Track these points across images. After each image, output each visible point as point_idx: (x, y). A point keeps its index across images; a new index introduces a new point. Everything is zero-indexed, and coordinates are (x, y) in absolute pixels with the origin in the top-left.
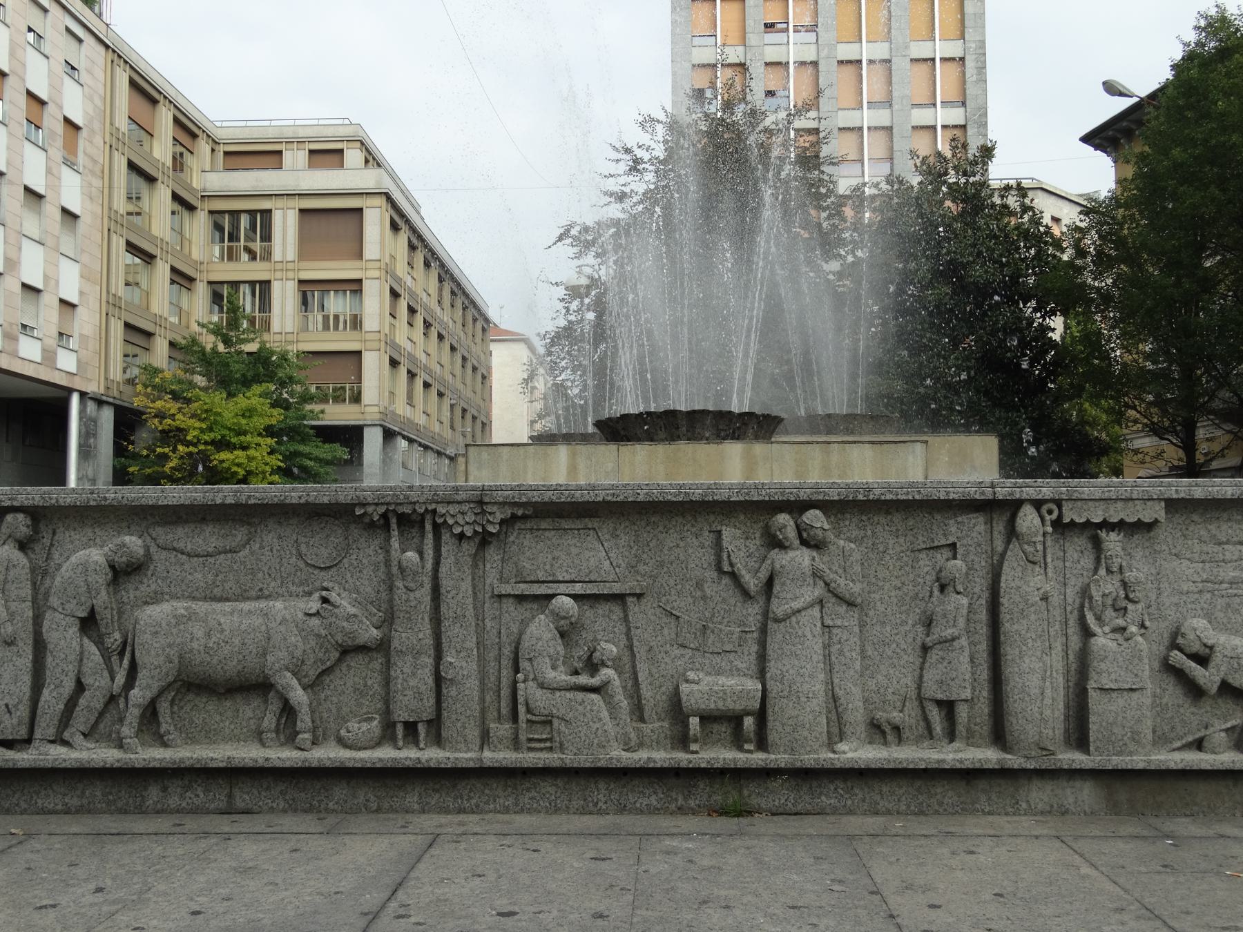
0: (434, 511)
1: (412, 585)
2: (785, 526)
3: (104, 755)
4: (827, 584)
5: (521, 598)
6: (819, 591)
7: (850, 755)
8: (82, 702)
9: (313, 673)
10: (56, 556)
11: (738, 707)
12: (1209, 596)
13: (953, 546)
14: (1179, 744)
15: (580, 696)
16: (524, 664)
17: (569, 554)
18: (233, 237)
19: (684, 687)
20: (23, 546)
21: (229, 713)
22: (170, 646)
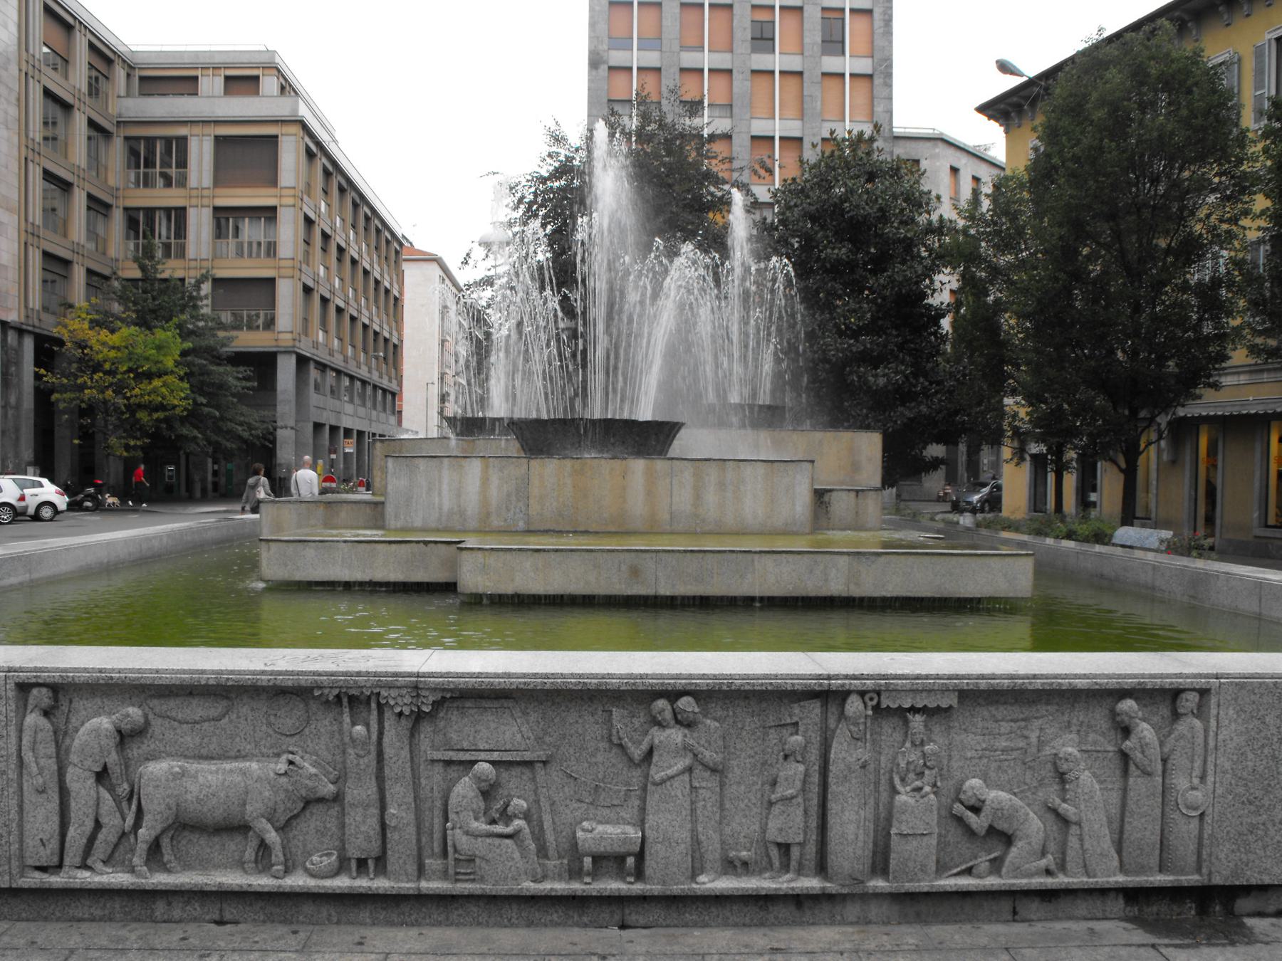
0: (379, 694)
1: (362, 753)
2: (664, 710)
4: (695, 755)
5: (448, 763)
6: (687, 761)
7: (709, 886)
8: (101, 836)
9: (283, 819)
10: (73, 720)
11: (622, 850)
12: (986, 760)
13: (796, 724)
14: (955, 871)
15: (497, 841)
16: (452, 816)
17: (488, 728)
18: (149, 163)
19: (580, 834)
20: (46, 713)
21: (217, 847)
22: (168, 796)
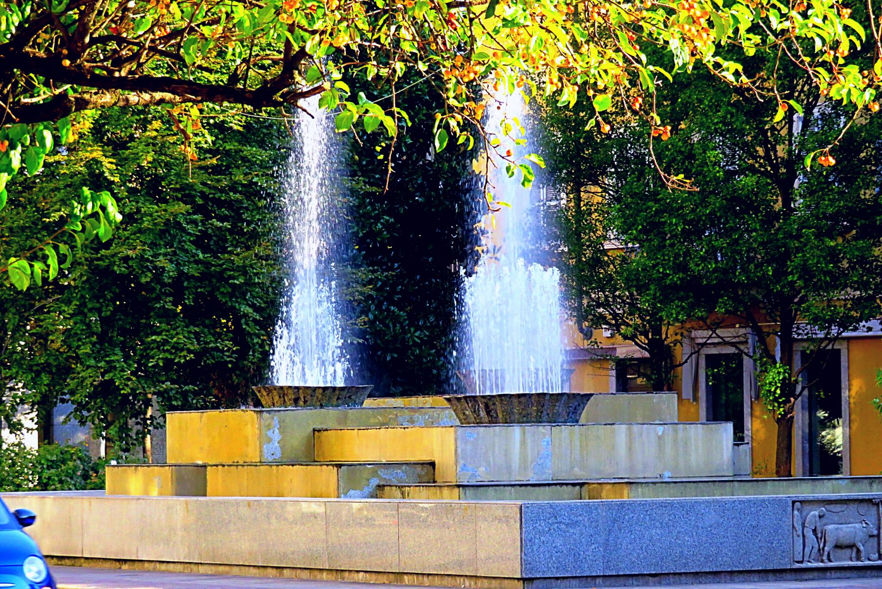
3: (821, 565)
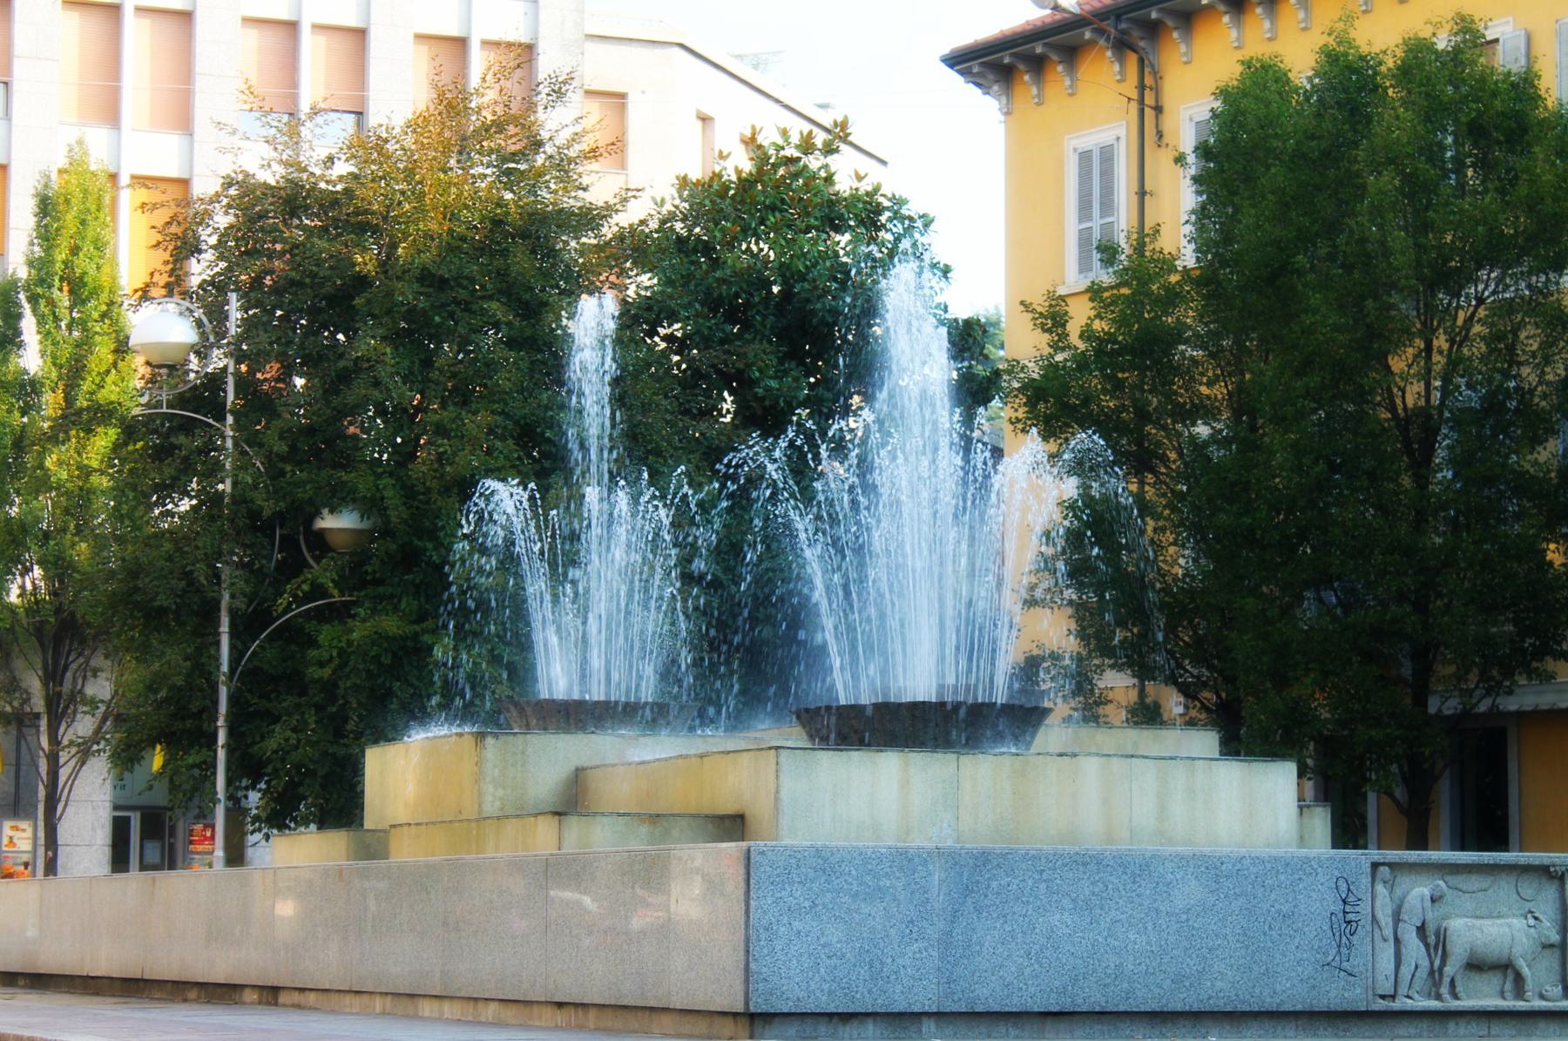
3: (1434, 1004)
